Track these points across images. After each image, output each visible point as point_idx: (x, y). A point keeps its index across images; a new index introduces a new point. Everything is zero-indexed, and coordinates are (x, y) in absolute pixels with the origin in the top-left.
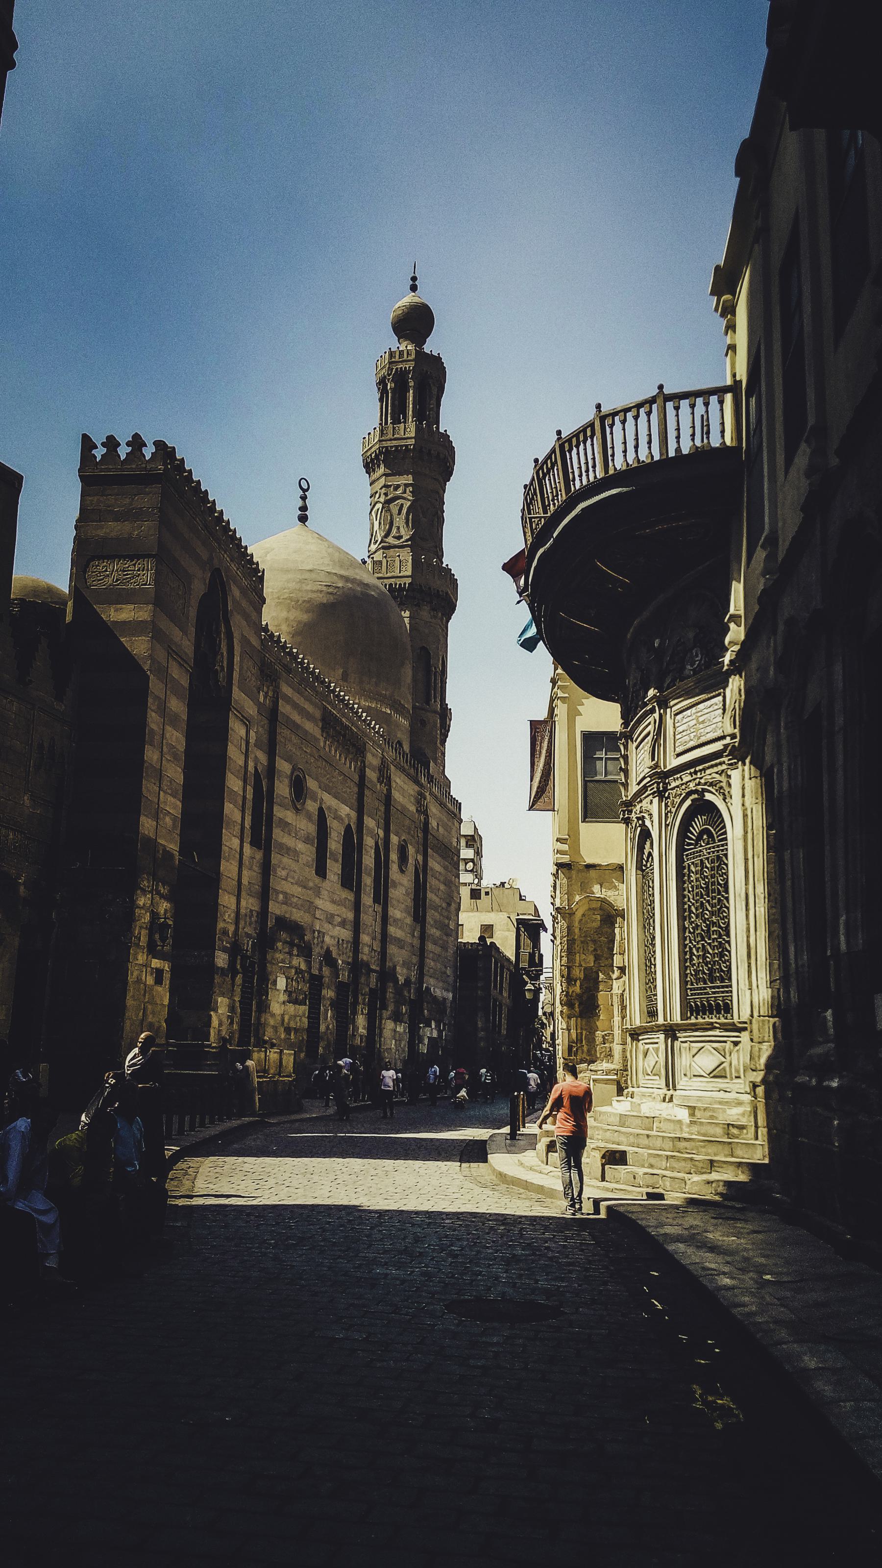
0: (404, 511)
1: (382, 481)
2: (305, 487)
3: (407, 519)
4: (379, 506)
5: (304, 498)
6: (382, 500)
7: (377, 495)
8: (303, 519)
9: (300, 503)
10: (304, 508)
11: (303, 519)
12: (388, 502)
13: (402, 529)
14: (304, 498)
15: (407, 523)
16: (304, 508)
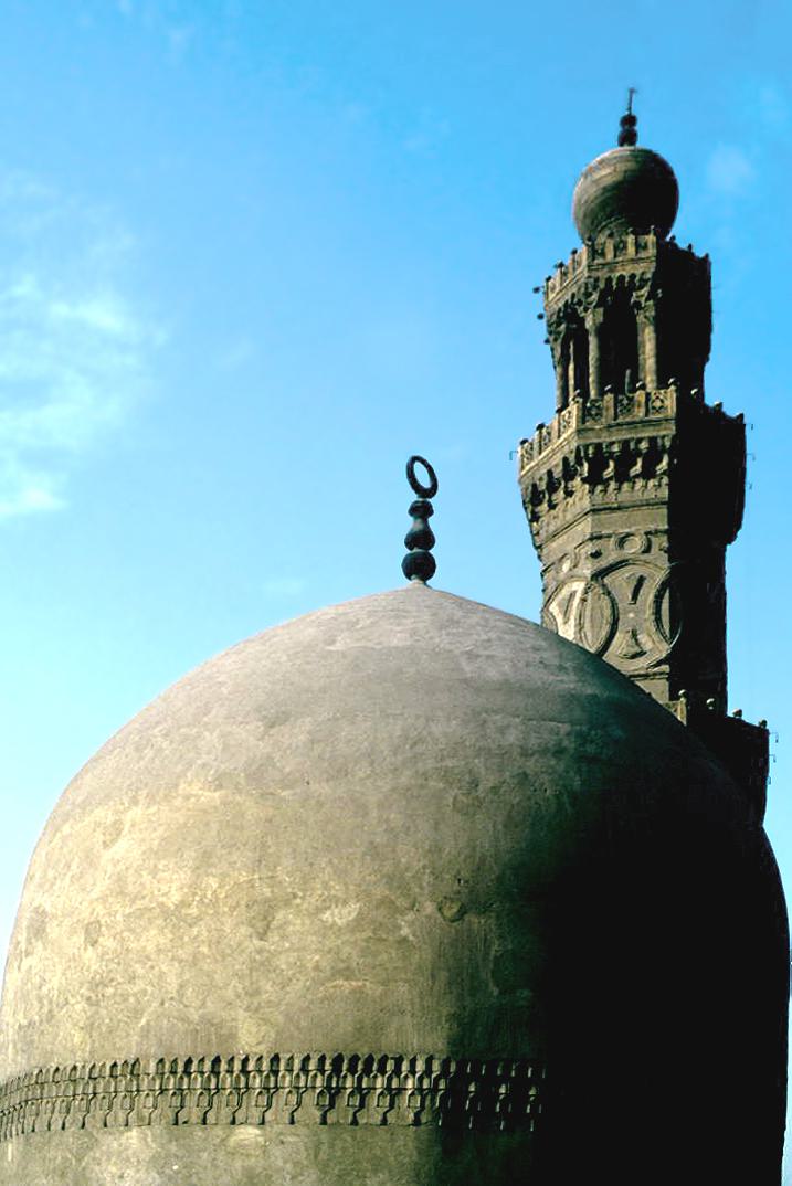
0: (648, 593)
1: (585, 527)
2: (425, 483)
3: (658, 612)
4: (579, 586)
5: (422, 511)
6: (587, 569)
7: (566, 566)
8: (420, 565)
9: (409, 524)
10: (421, 540)
11: (420, 565)
12: (599, 575)
13: (642, 638)
14: (422, 511)
15: (658, 620)
16: (421, 540)
